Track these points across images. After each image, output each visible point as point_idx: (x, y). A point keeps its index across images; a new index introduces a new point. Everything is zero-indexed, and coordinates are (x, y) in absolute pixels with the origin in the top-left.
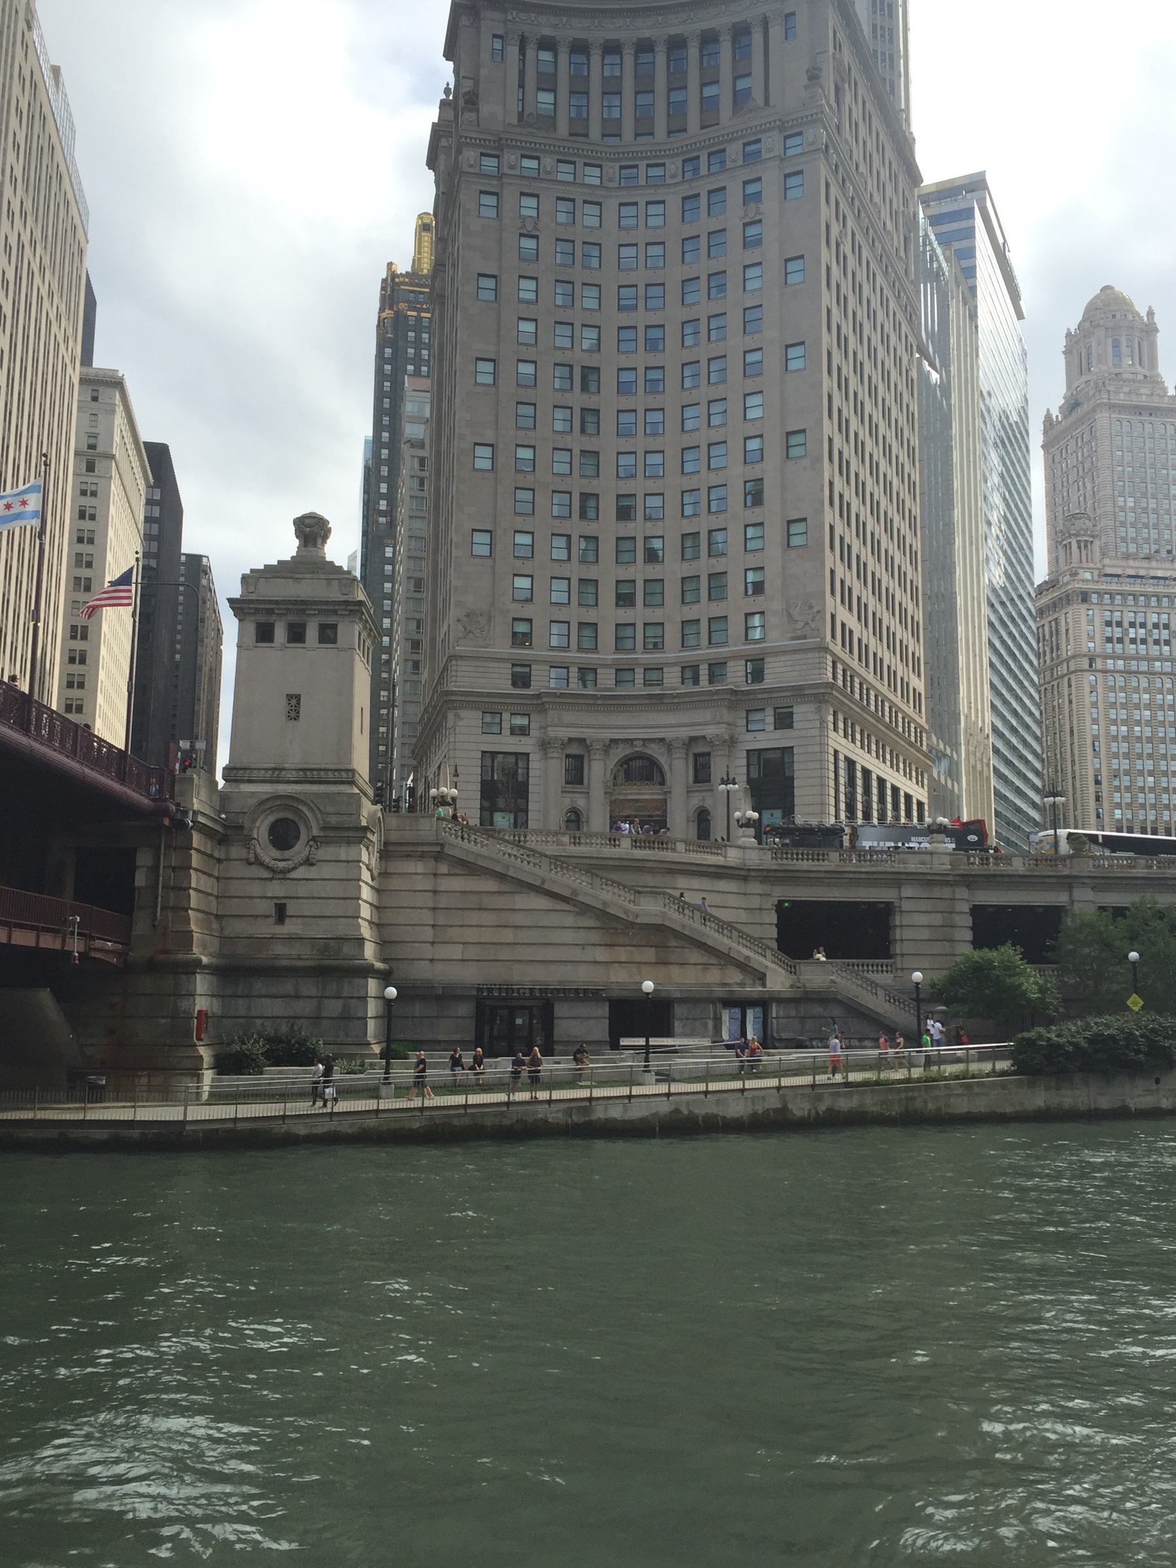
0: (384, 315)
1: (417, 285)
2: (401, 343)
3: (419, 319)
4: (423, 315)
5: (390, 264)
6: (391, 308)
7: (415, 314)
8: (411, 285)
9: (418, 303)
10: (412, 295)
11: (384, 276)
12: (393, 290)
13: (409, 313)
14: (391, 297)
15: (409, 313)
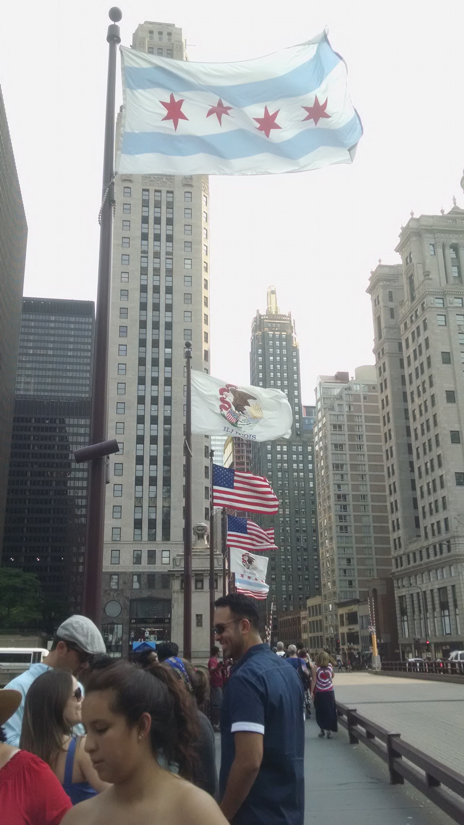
0: (257, 334)
1: (272, 319)
2: (266, 346)
3: (274, 335)
4: (276, 333)
5: (258, 311)
6: (260, 330)
7: (272, 333)
8: (269, 319)
9: (273, 328)
10: (270, 324)
11: (255, 316)
12: (260, 322)
13: (269, 333)
14: (260, 325)
15: (269, 333)
